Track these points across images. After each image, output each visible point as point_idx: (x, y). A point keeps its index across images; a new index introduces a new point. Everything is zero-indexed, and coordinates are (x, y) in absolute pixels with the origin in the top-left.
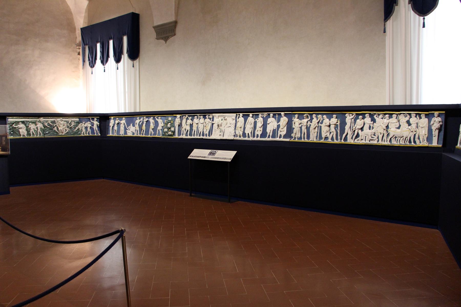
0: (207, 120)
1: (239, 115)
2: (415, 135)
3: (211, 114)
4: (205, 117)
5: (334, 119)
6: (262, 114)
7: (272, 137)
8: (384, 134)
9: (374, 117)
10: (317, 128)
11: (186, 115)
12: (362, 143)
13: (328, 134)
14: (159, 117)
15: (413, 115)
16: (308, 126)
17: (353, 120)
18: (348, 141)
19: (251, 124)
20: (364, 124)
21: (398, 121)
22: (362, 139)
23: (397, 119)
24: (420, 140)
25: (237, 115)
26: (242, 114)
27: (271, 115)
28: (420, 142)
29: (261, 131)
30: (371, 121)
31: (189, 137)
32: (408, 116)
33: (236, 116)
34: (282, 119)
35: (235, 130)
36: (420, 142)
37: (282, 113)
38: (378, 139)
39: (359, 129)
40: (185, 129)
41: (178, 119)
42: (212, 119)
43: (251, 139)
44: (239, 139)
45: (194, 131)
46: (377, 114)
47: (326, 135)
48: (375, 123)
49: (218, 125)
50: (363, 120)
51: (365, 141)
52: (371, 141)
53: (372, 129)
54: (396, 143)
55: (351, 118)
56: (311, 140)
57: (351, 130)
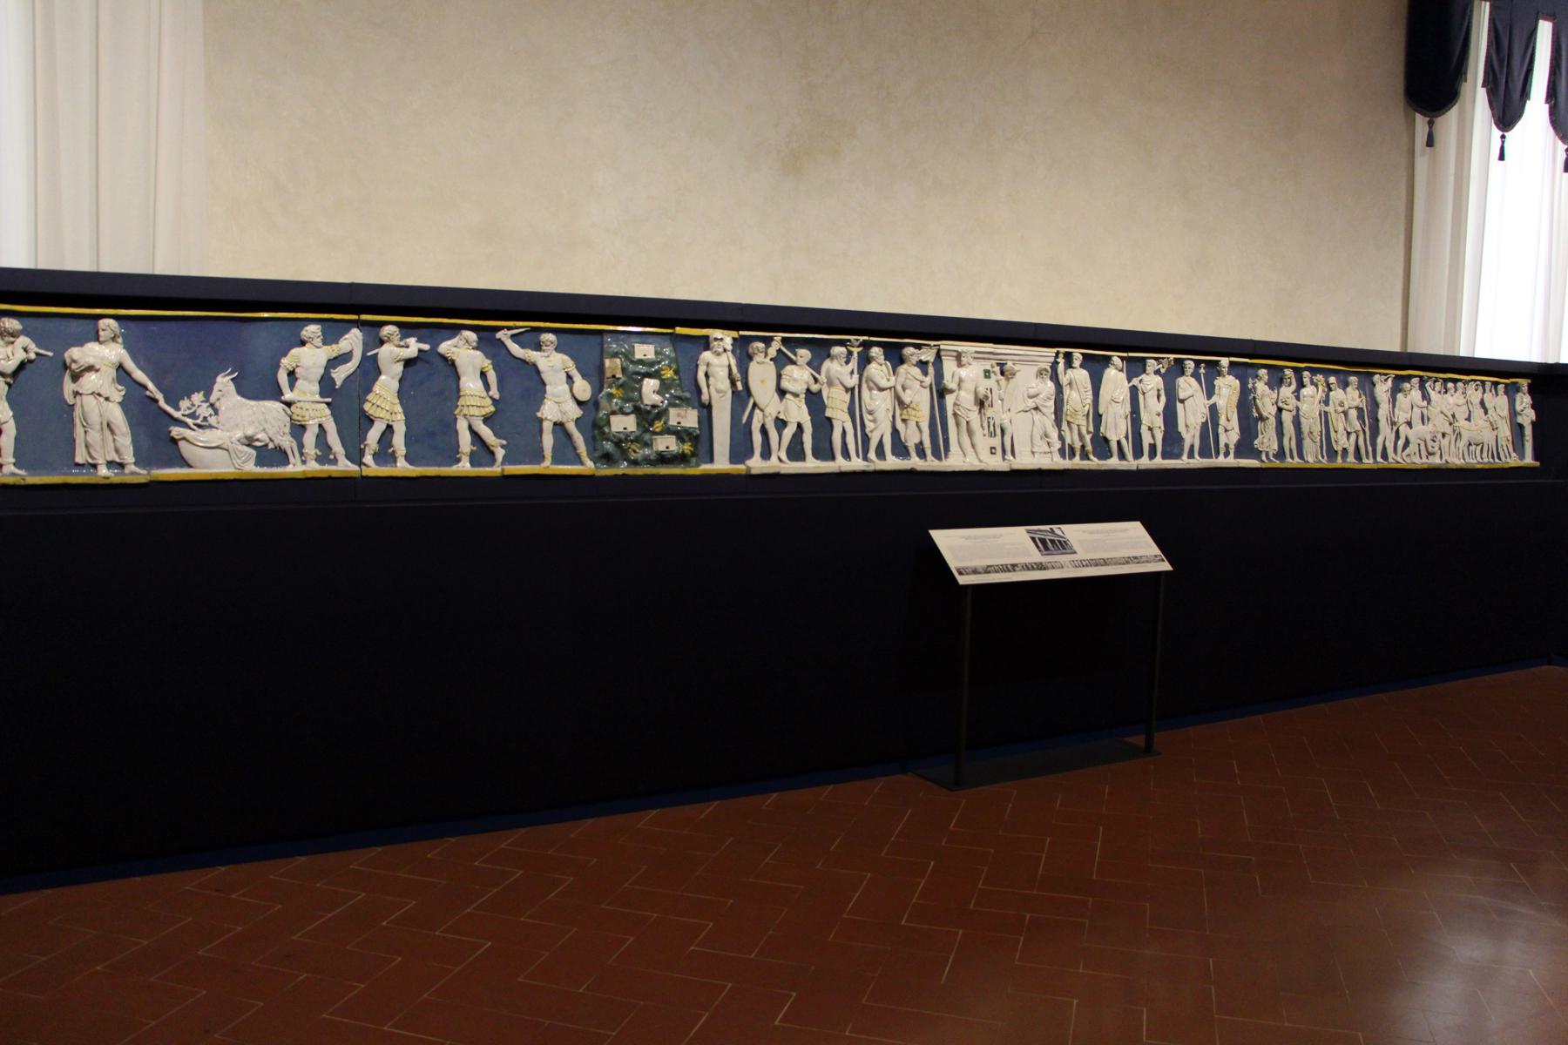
0: (909, 371)
3: (932, 343)
4: (895, 357)
6: (1156, 359)
7: (1202, 455)
12: (1422, 464)
26: (1082, 354)
27: (1190, 365)
31: (811, 465)
33: (1052, 360)
37: (1225, 361)
42: (931, 370)
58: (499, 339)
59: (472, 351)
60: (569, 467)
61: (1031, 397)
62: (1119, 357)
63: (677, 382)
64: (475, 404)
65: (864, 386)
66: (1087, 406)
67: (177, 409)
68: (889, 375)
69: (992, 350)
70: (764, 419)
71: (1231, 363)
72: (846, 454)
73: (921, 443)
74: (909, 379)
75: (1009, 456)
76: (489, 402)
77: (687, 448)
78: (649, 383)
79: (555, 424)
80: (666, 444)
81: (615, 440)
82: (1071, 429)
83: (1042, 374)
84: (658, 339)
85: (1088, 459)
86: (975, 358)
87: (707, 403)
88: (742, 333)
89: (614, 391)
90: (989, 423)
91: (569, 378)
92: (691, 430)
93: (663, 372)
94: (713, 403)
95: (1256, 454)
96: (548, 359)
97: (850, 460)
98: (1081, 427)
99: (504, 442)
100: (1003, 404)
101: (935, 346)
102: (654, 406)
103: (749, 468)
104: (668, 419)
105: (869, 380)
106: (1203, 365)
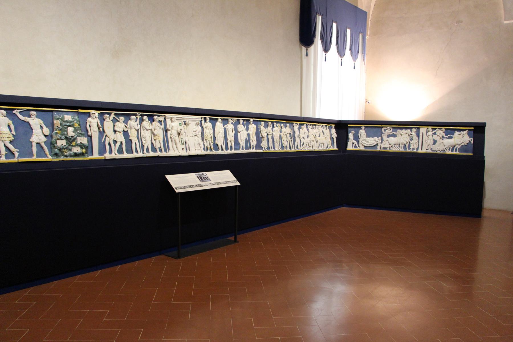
0: (156, 124)
3: (163, 115)
6: (231, 119)
11: (111, 113)
26: (209, 118)
27: (241, 121)
31: (126, 155)
33: (200, 120)
37: (252, 120)
42: (163, 123)
58: (15, 113)
59: (4, 118)
60: (41, 158)
61: (194, 132)
62: (220, 119)
63: (80, 128)
64: (6, 137)
65: (142, 129)
66: (211, 134)
68: (150, 125)
69: (182, 117)
70: (109, 140)
71: (254, 120)
72: (137, 151)
73: (160, 147)
74: (156, 127)
75: (188, 151)
76: (12, 136)
77: (84, 151)
78: (70, 129)
79: (37, 143)
80: (77, 149)
81: (59, 149)
82: (206, 141)
83: (197, 124)
84: (73, 113)
85: (212, 151)
86: (177, 119)
87: (90, 135)
88: (101, 111)
89: (58, 131)
90: (181, 140)
91: (41, 127)
92: (85, 145)
93: (74, 125)
94: (92, 135)
95: (261, 148)
96: (34, 120)
97: (149, 153)
98: (210, 141)
99: (18, 150)
100: (185, 134)
101: (164, 115)
102: (72, 137)
103: (105, 157)
104: (77, 141)
105: (143, 127)
106: (245, 121)
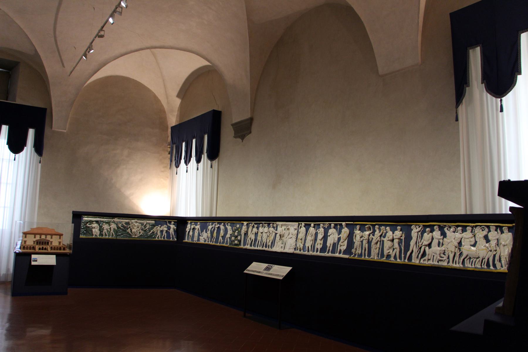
1: (301, 224)
2: (494, 256)
3: (275, 223)
5: (399, 233)
6: (323, 224)
7: (332, 253)
8: (455, 253)
9: (444, 230)
10: (379, 242)
12: (428, 264)
13: (391, 251)
14: (229, 224)
15: (493, 229)
16: (370, 240)
17: (420, 233)
18: (413, 261)
19: (312, 235)
20: (433, 239)
21: (473, 235)
22: (429, 258)
23: (473, 233)
24: (501, 263)
25: (299, 224)
26: (305, 224)
27: (333, 225)
28: (502, 266)
29: (321, 245)
30: (441, 236)
31: (253, 248)
32: (487, 230)
33: (298, 225)
34: (343, 230)
35: (296, 242)
36: (502, 266)
37: (344, 223)
38: (448, 260)
39: (426, 245)
40: (251, 238)
41: (244, 226)
42: (275, 228)
43: (311, 253)
44: (299, 253)
45: (258, 241)
46: (447, 226)
47: (388, 252)
48: (446, 238)
49: (280, 235)
50: (431, 234)
51: (433, 262)
52: (439, 262)
53: (442, 246)
54: (470, 266)
55: (418, 231)
56: (372, 258)
57: (417, 247)
67: (201, 234)
71: (346, 224)
95: (351, 253)
